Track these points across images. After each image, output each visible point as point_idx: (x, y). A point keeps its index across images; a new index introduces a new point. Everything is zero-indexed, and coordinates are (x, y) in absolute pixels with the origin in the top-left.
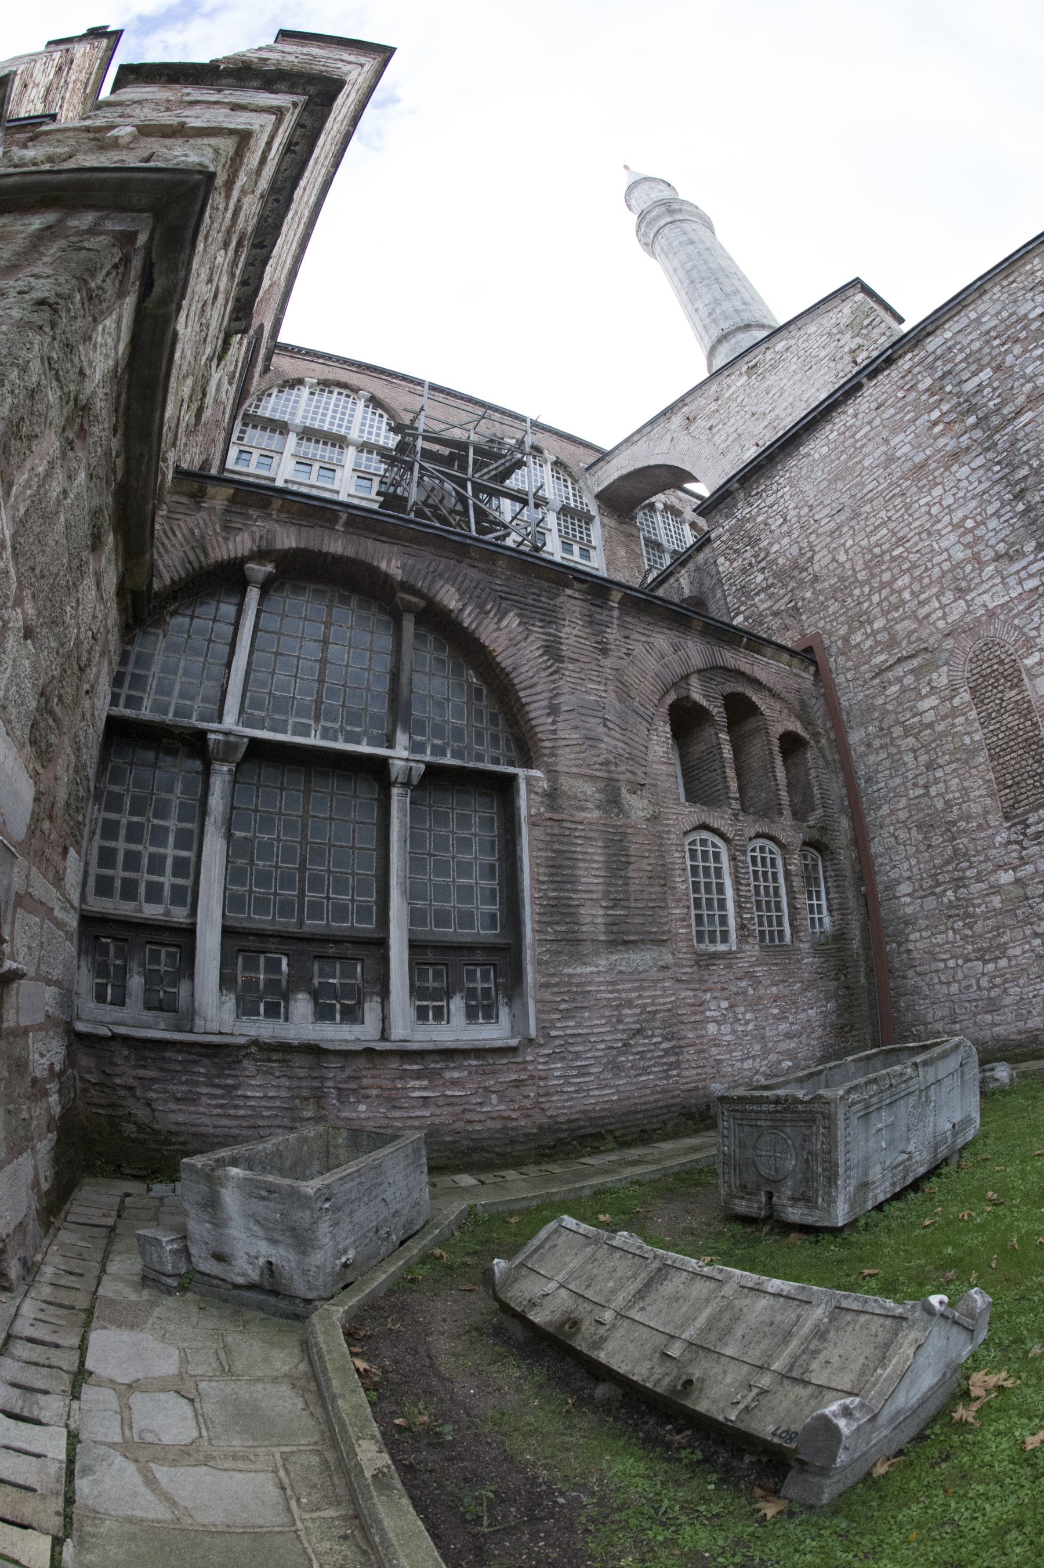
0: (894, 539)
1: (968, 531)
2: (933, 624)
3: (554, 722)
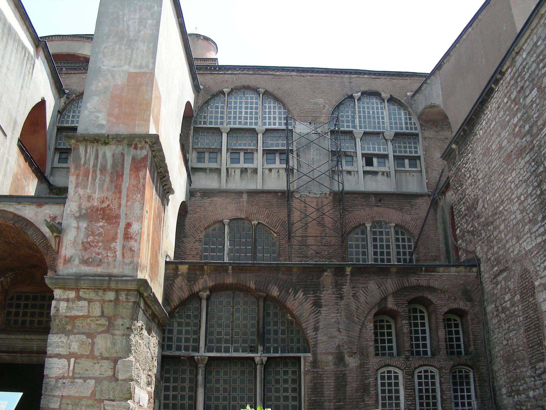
0: (500, 201)
1: (522, 203)
2: (510, 254)
3: (316, 334)
